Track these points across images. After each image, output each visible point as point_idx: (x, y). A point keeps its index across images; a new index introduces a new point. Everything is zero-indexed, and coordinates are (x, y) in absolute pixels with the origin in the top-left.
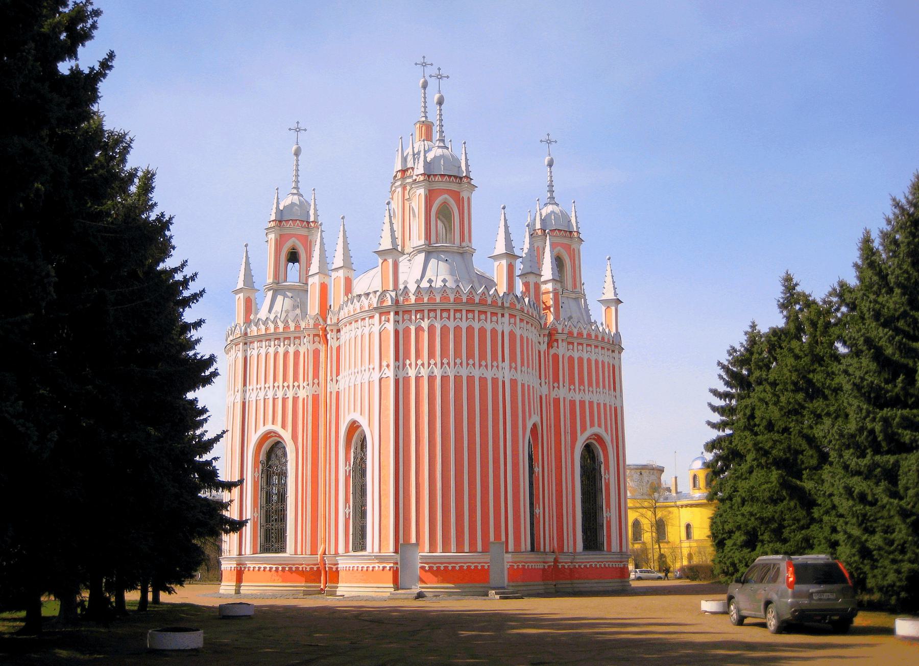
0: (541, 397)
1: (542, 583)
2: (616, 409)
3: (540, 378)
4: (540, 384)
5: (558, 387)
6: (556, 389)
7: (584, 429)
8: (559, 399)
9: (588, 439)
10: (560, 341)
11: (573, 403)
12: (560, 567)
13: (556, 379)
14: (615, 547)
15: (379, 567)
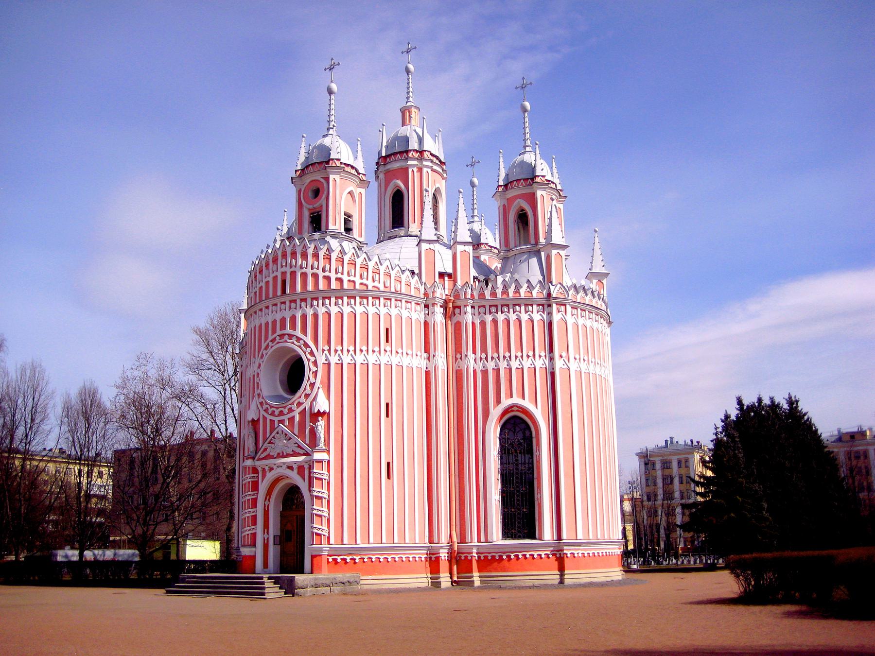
0: (428, 373)
1: (429, 575)
2: (553, 375)
3: (427, 350)
4: (429, 359)
5: (461, 358)
6: (459, 360)
7: (498, 401)
8: (462, 369)
9: (506, 412)
10: (462, 307)
11: (485, 373)
12: (463, 558)
13: (458, 349)
14: (548, 533)
15: (609, 552)
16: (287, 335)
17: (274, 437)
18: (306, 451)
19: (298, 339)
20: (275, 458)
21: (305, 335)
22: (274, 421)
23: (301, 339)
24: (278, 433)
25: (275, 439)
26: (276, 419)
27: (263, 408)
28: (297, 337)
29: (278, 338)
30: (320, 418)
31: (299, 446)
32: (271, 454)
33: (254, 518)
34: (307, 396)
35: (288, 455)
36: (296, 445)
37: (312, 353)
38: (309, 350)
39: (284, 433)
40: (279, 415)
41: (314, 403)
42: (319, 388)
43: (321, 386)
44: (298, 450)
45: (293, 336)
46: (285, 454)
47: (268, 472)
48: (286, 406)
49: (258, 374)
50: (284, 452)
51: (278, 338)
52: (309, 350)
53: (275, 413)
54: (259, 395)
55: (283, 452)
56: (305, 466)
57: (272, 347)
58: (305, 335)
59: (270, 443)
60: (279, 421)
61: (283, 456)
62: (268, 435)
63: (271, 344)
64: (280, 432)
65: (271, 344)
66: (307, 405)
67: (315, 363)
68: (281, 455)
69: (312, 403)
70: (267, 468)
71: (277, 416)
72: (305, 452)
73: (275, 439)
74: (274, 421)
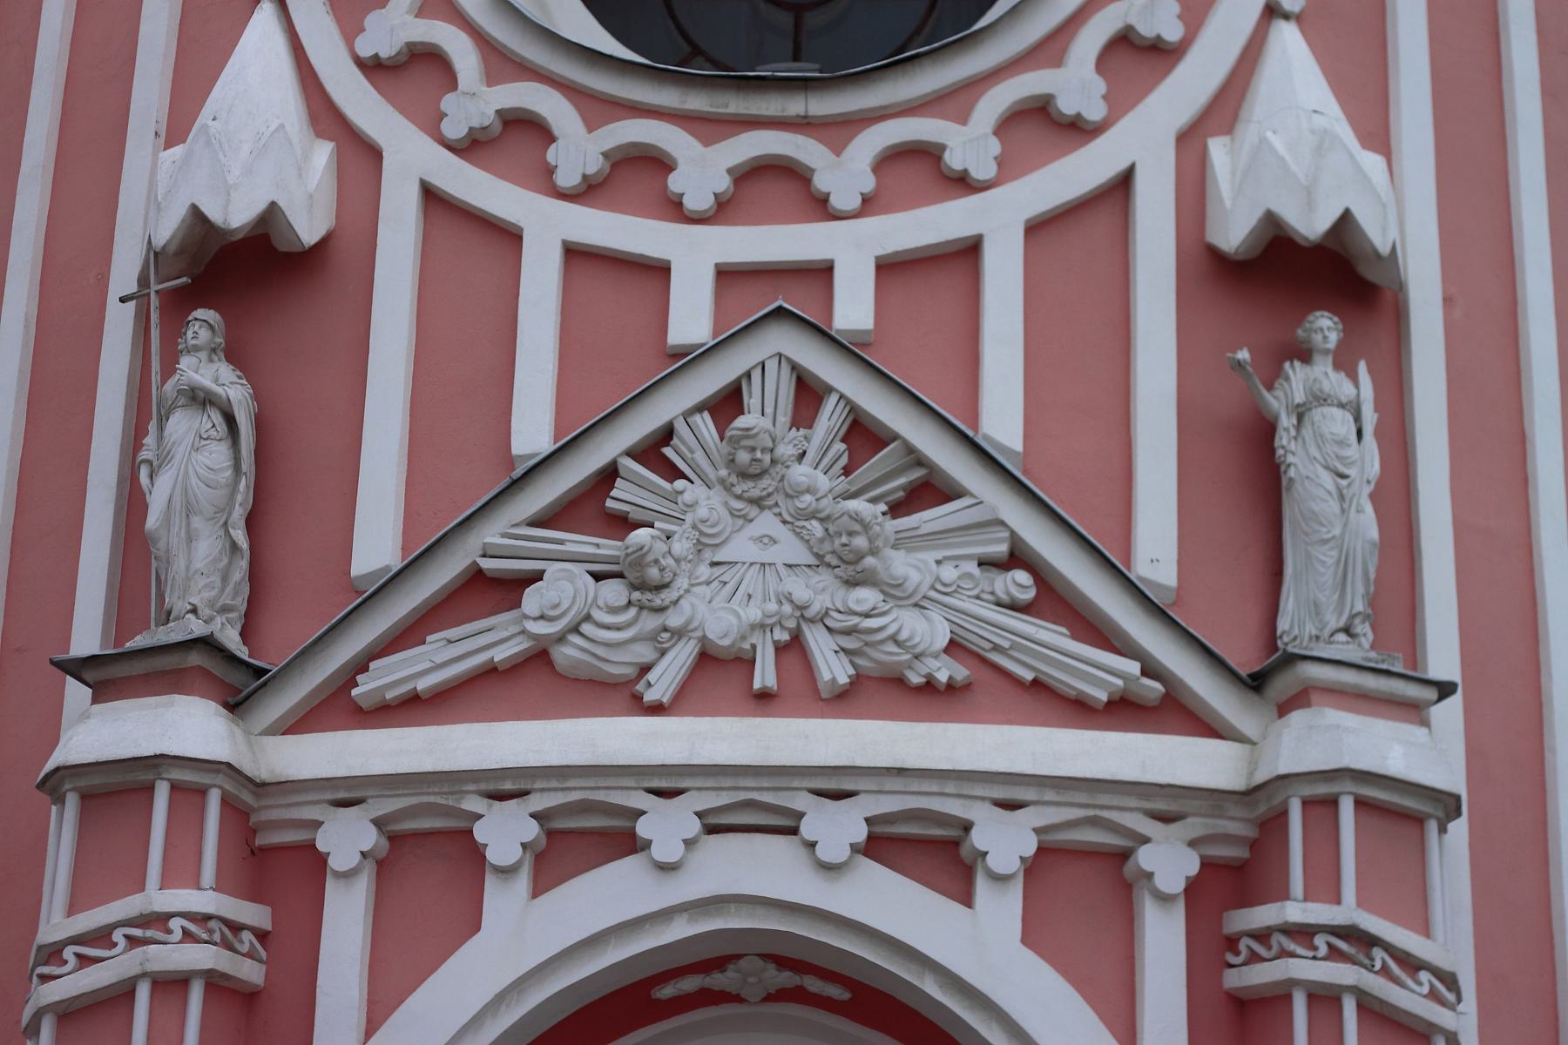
18: (1151, 669)
20: (657, 709)
22: (659, 271)
24: (727, 404)
25: (673, 473)
27: (432, 125)
30: (1325, 327)
32: (567, 654)
36: (1020, 583)
39: (829, 418)
41: (1217, 148)
46: (833, 669)
47: (523, 882)
50: (820, 645)
53: (676, 182)
55: (793, 649)
56: (1146, 858)
60: (727, 275)
68: (765, 675)
73: (673, 473)
74: (659, 271)
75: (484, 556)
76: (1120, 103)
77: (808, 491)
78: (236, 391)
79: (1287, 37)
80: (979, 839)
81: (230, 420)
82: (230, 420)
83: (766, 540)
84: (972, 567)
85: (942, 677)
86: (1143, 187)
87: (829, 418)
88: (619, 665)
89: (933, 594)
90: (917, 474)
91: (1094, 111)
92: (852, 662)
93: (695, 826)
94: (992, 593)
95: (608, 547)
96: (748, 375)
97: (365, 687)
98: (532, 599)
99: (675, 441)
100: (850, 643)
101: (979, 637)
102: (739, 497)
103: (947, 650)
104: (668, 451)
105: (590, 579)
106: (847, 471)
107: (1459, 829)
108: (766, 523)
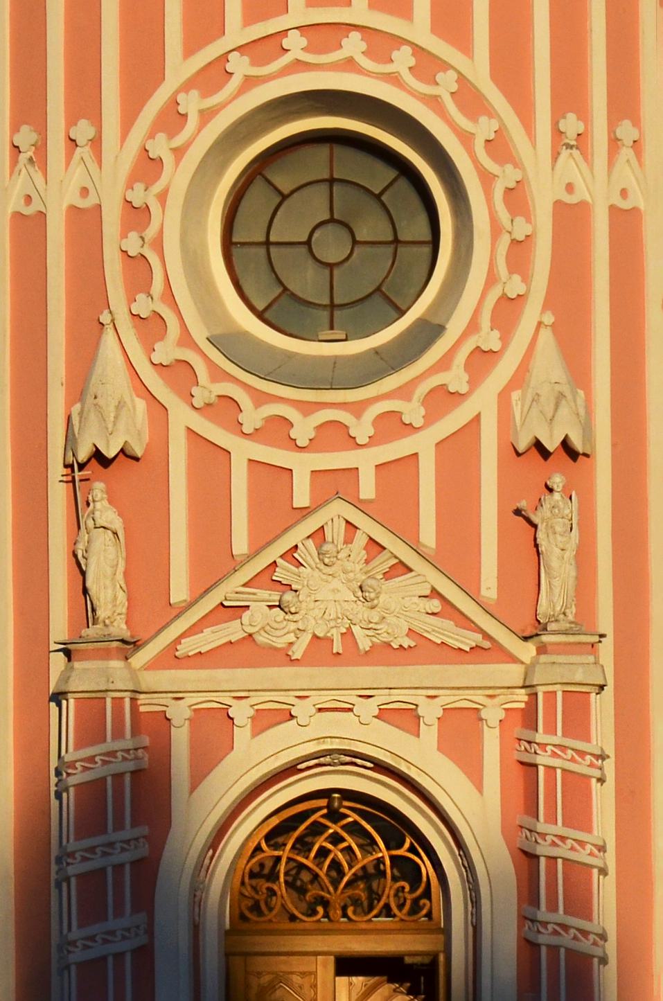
16: (355, 36)
17: (290, 554)
18: (487, 636)
19: (427, 65)
21: (464, 45)
23: (445, 66)
24: (319, 535)
26: (303, 466)
28: (418, 50)
29: (295, 42)
31: (449, 610)
32: (261, 639)
33: (144, 955)
34: (482, 360)
35: (385, 653)
36: (435, 605)
37: (499, 147)
38: (484, 129)
39: (360, 540)
40: (313, 446)
41: (515, 395)
42: (540, 323)
43: (549, 319)
44: (444, 631)
45: (402, 41)
46: (364, 644)
48: (357, 409)
49: (136, 216)
51: (295, 42)
52: (484, 129)
54: (151, 328)
55: (348, 635)
57: (250, 82)
58: (464, 45)
59: (267, 577)
61: (350, 654)
62: (240, 545)
63: (240, 66)
64: (336, 532)
65: (240, 66)
66: (484, 402)
67: (517, 198)
69: (504, 398)
70: (241, 713)
71: (301, 449)
72: (487, 644)
75: (226, 599)
76: (474, 383)
77: (351, 571)
78: (118, 524)
79: (546, 336)
80: (420, 711)
81: (115, 533)
82: (115, 533)
83: (336, 591)
84: (416, 600)
85: (406, 646)
86: (484, 421)
87: (360, 540)
88: (280, 643)
89: (402, 612)
90: (395, 561)
91: (464, 389)
92: (371, 641)
93: (314, 710)
94: (425, 609)
95: (275, 597)
96: (327, 523)
97: (182, 650)
98: (246, 616)
99: (299, 551)
100: (370, 633)
101: (418, 627)
102: (324, 574)
103: (407, 635)
104: (296, 555)
105: (267, 608)
106: (367, 562)
107: (609, 690)
108: (336, 583)
